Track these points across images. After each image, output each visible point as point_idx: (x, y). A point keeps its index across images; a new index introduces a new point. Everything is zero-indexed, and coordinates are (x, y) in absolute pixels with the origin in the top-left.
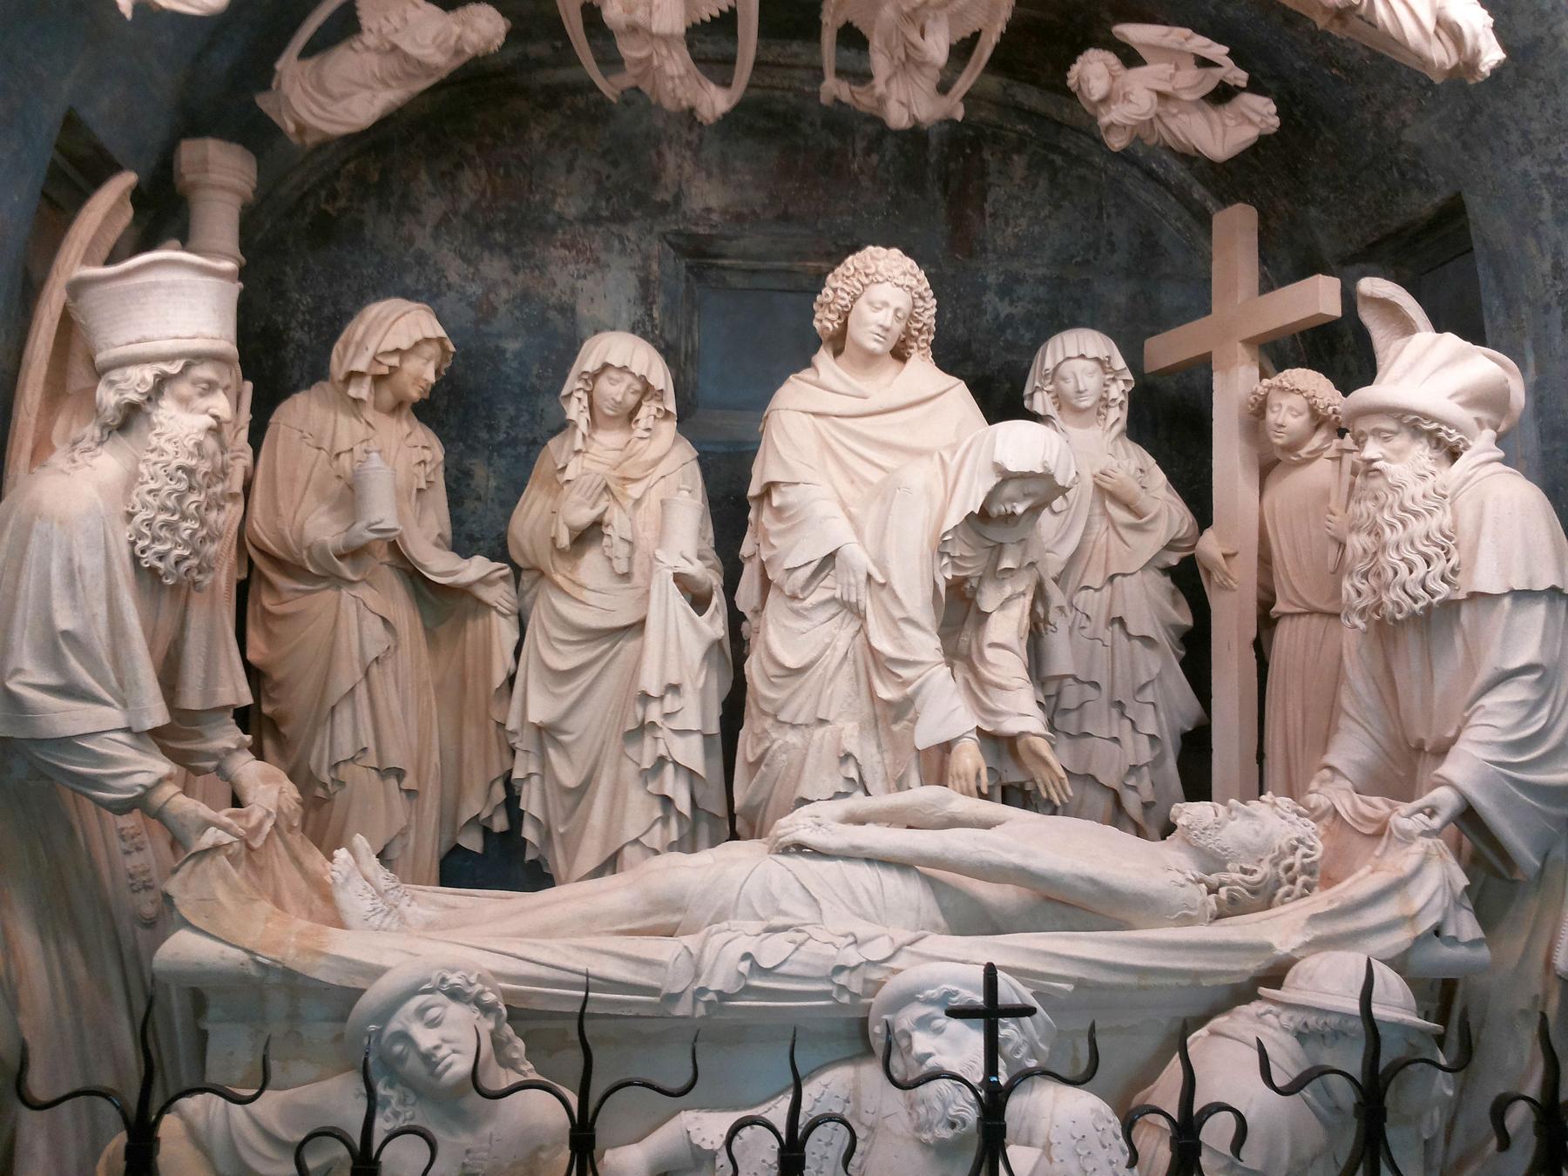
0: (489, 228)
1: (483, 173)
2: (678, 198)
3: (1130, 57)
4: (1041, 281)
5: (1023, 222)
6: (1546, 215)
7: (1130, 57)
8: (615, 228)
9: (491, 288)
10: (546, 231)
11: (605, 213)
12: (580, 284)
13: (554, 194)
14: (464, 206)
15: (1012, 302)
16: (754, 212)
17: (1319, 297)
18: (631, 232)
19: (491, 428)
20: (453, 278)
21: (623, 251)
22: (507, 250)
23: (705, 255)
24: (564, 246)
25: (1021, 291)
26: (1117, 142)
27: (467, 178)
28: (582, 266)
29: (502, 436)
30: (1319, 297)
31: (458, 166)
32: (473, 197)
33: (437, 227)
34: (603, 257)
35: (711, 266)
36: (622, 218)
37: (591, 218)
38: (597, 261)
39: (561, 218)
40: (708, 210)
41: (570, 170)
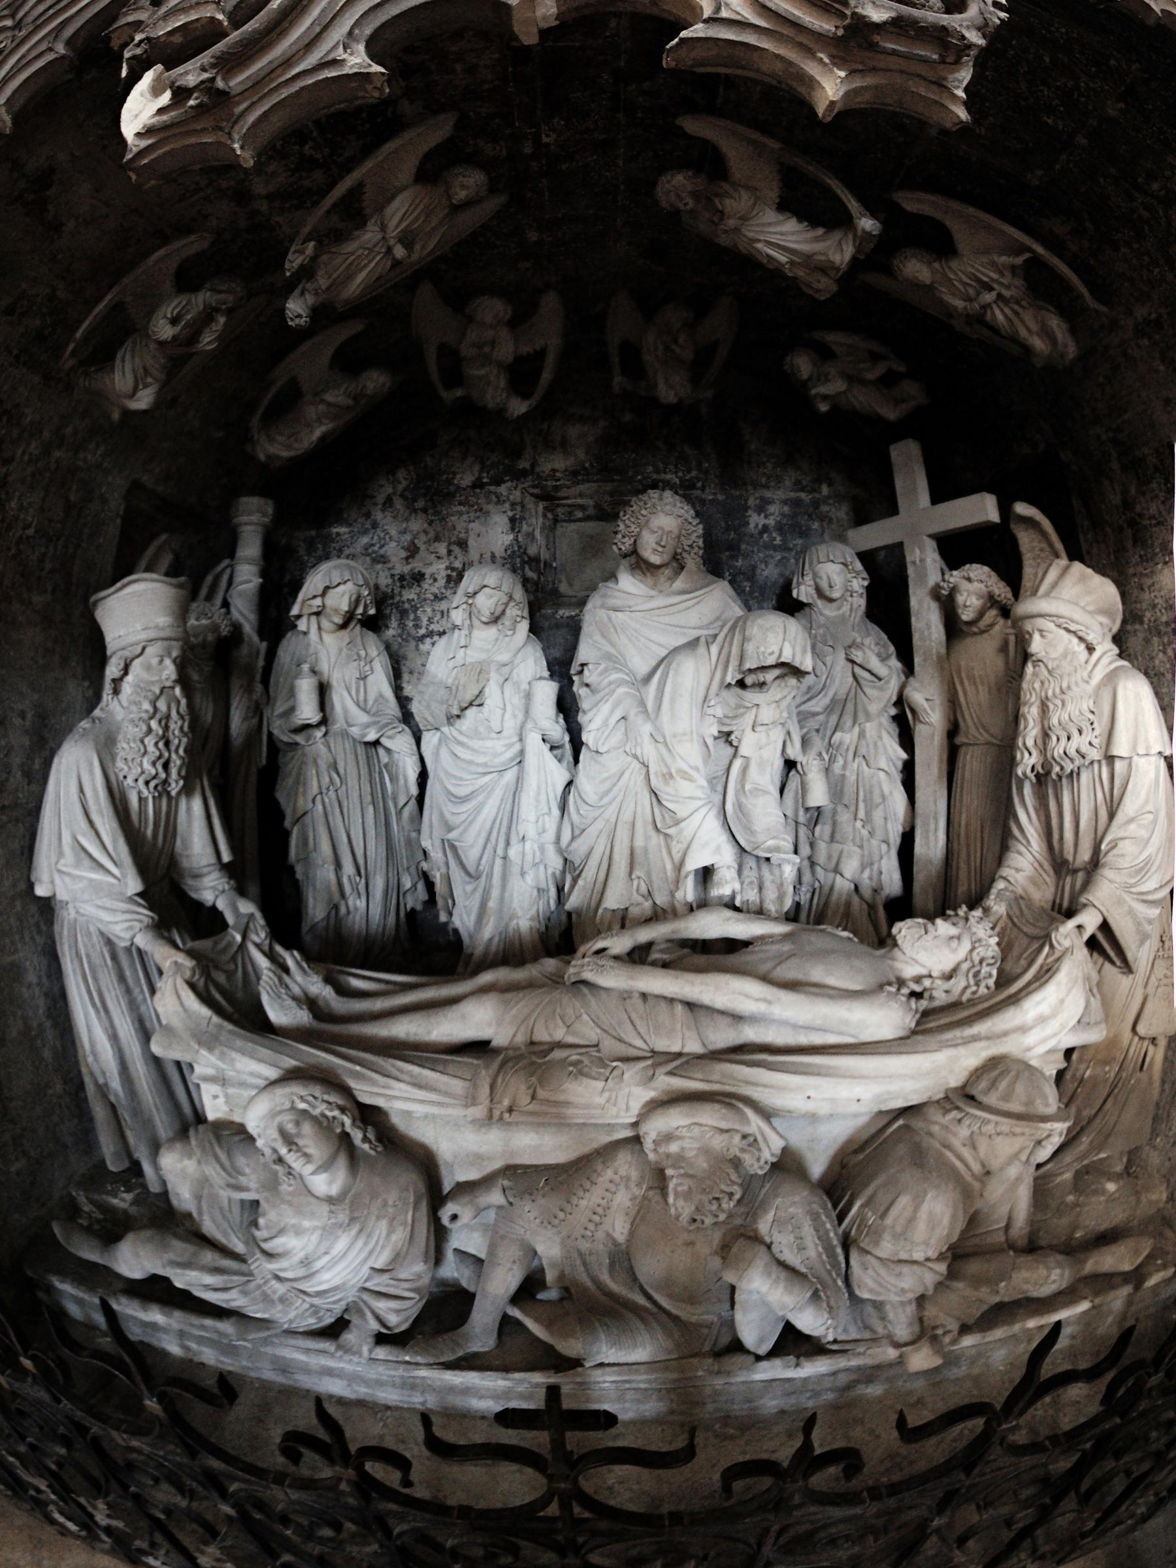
0: (415, 500)
2: (533, 466)
4: (785, 502)
5: (769, 466)
6: (1115, 465)
8: (492, 488)
9: (415, 537)
10: (449, 496)
12: (472, 525)
13: (455, 474)
14: (400, 487)
17: (982, 508)
18: (503, 489)
20: (393, 532)
22: (425, 511)
23: (553, 498)
25: (772, 508)
28: (472, 515)
30: (982, 508)
32: (405, 483)
33: (384, 504)
34: (486, 507)
36: (498, 482)
39: (458, 487)
40: (554, 470)
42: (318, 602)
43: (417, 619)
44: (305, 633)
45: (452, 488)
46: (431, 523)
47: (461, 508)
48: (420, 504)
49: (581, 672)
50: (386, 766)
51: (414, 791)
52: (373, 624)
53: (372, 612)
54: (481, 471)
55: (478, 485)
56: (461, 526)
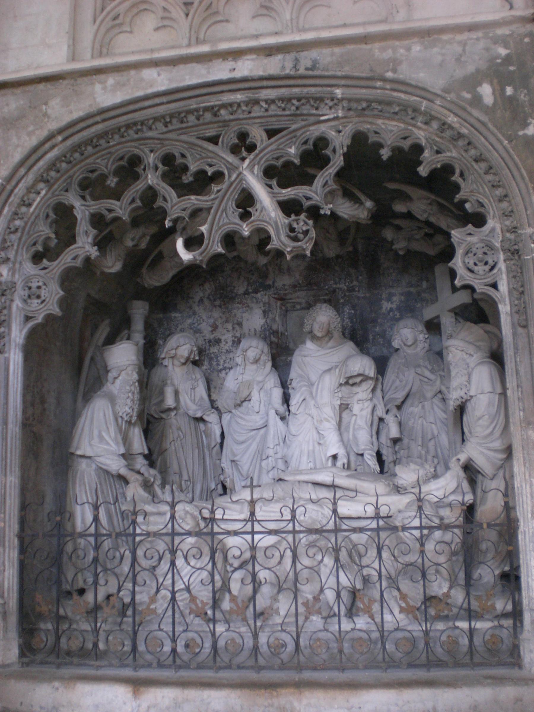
0: (215, 300)
1: (212, 283)
2: (274, 283)
3: (399, 228)
7: (399, 228)
8: (254, 295)
9: (216, 320)
10: (232, 299)
11: (250, 291)
12: (244, 315)
13: (234, 287)
15: (392, 303)
16: (299, 284)
18: (259, 295)
19: (218, 365)
20: (204, 318)
21: (257, 302)
22: (220, 306)
24: (238, 303)
26: (401, 253)
27: (207, 286)
28: (244, 309)
29: (221, 367)
31: (205, 282)
32: (209, 291)
33: (199, 302)
34: (251, 305)
35: (287, 303)
36: (256, 291)
37: (246, 293)
38: (248, 306)
39: (237, 295)
40: (284, 285)
41: (239, 278)
42: (173, 352)
43: (218, 361)
44: (166, 366)
45: (234, 295)
46: (223, 313)
47: (238, 305)
48: (218, 303)
49: (291, 384)
50: (204, 431)
51: (219, 440)
52: (195, 363)
53: (197, 358)
54: (248, 286)
55: (246, 293)
56: (239, 314)
